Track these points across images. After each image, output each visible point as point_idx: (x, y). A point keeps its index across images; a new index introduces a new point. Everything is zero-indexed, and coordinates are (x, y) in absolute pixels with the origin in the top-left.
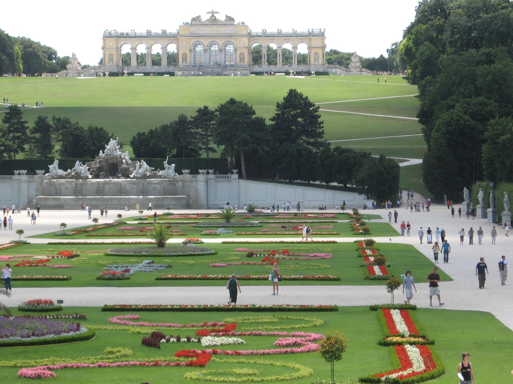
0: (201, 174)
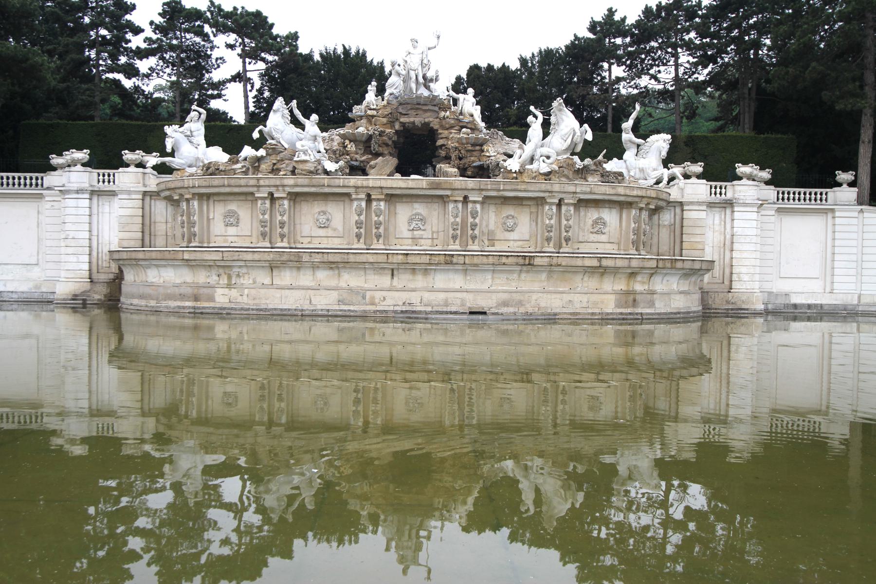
0: (744, 181)
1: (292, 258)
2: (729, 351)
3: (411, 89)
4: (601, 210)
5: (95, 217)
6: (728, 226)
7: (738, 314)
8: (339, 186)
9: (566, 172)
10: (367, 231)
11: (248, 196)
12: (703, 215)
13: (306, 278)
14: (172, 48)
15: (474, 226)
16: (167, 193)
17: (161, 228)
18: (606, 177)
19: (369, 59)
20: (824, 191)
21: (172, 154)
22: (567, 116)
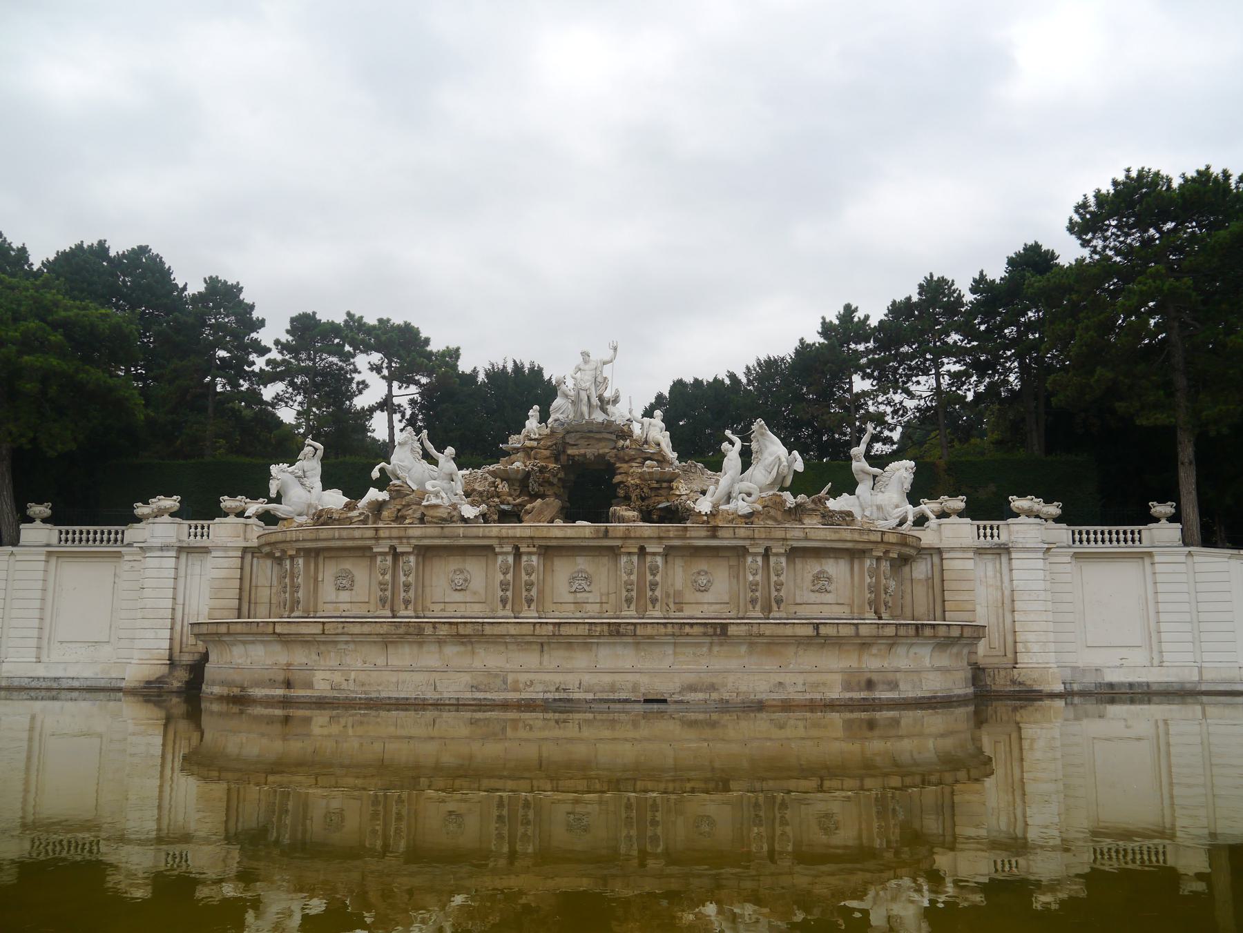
0: (1023, 519)
1: (411, 630)
2: (1021, 749)
3: (582, 414)
4: (823, 561)
5: (181, 581)
6: (1006, 579)
7: (1028, 696)
8: (478, 537)
9: (773, 512)
10: (515, 594)
11: (364, 552)
12: (970, 564)
13: (430, 658)
14: (304, 371)
15: (654, 586)
16: (267, 549)
17: (264, 594)
18: (828, 517)
19: (546, 377)
20: (1136, 528)
21: (278, 499)
22: (772, 442)
